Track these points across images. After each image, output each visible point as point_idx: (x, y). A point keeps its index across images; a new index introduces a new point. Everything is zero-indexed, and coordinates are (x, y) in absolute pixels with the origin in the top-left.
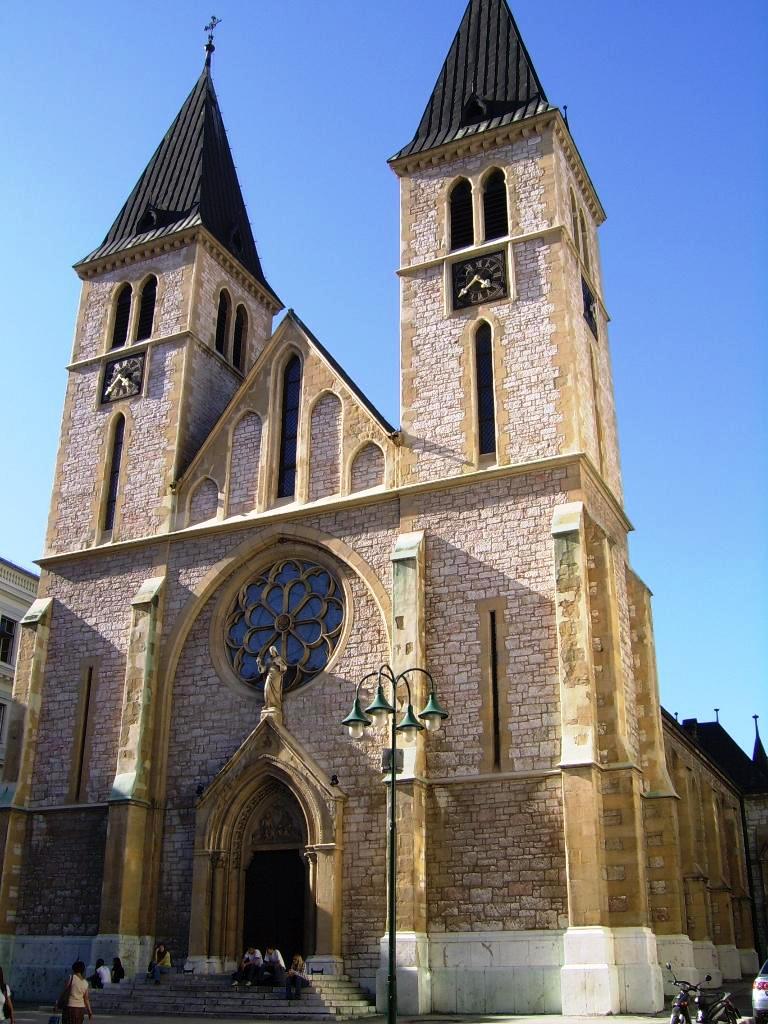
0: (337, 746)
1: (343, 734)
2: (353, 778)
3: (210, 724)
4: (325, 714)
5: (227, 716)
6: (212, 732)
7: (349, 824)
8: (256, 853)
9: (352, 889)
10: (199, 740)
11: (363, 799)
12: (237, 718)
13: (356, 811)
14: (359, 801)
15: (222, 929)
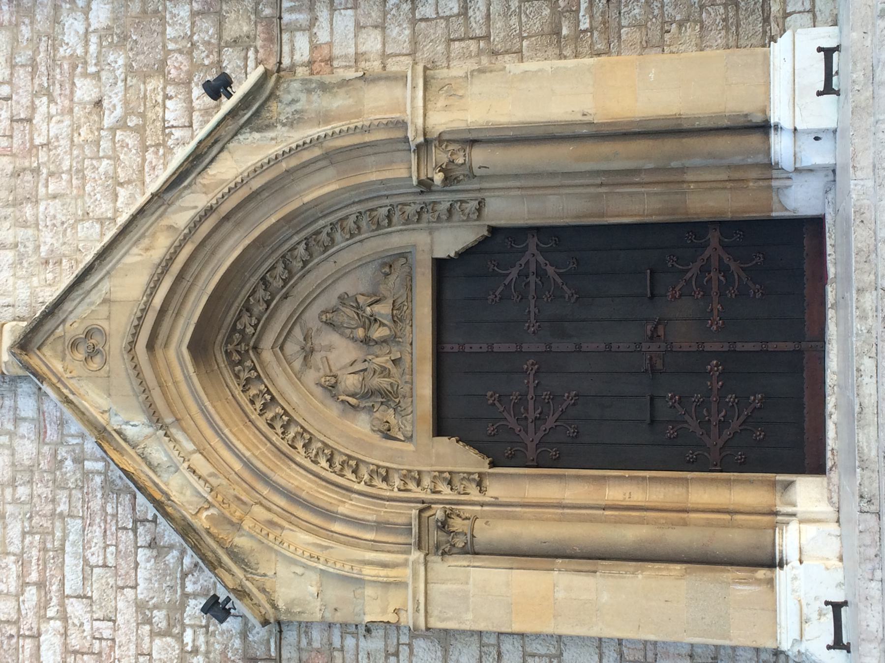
0: (133, 121)
1: (99, 103)
2: (228, 52)
3: (31, 595)
4: (36, 171)
5: (14, 531)
6: (54, 588)
7: (359, 57)
8: (439, 430)
9: (558, 33)
10: (75, 641)
11: (286, 17)
12: (23, 492)
13: (323, 36)
14: (295, 28)
15: (685, 524)
